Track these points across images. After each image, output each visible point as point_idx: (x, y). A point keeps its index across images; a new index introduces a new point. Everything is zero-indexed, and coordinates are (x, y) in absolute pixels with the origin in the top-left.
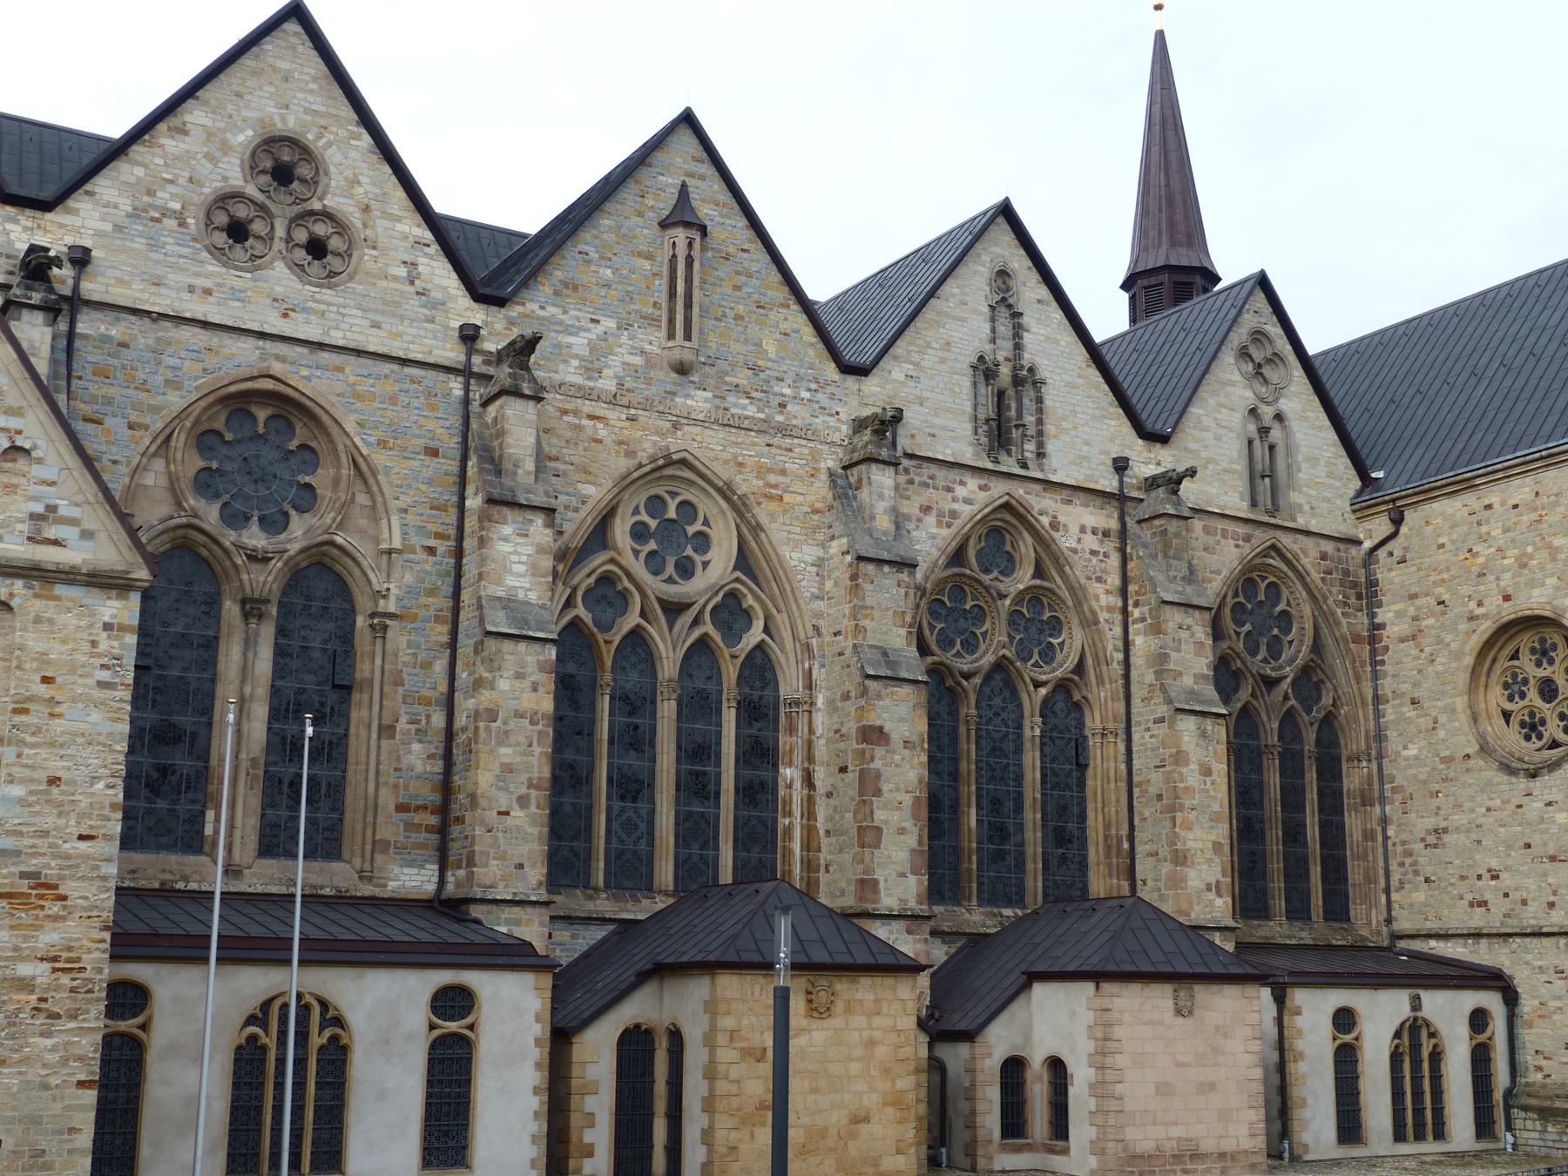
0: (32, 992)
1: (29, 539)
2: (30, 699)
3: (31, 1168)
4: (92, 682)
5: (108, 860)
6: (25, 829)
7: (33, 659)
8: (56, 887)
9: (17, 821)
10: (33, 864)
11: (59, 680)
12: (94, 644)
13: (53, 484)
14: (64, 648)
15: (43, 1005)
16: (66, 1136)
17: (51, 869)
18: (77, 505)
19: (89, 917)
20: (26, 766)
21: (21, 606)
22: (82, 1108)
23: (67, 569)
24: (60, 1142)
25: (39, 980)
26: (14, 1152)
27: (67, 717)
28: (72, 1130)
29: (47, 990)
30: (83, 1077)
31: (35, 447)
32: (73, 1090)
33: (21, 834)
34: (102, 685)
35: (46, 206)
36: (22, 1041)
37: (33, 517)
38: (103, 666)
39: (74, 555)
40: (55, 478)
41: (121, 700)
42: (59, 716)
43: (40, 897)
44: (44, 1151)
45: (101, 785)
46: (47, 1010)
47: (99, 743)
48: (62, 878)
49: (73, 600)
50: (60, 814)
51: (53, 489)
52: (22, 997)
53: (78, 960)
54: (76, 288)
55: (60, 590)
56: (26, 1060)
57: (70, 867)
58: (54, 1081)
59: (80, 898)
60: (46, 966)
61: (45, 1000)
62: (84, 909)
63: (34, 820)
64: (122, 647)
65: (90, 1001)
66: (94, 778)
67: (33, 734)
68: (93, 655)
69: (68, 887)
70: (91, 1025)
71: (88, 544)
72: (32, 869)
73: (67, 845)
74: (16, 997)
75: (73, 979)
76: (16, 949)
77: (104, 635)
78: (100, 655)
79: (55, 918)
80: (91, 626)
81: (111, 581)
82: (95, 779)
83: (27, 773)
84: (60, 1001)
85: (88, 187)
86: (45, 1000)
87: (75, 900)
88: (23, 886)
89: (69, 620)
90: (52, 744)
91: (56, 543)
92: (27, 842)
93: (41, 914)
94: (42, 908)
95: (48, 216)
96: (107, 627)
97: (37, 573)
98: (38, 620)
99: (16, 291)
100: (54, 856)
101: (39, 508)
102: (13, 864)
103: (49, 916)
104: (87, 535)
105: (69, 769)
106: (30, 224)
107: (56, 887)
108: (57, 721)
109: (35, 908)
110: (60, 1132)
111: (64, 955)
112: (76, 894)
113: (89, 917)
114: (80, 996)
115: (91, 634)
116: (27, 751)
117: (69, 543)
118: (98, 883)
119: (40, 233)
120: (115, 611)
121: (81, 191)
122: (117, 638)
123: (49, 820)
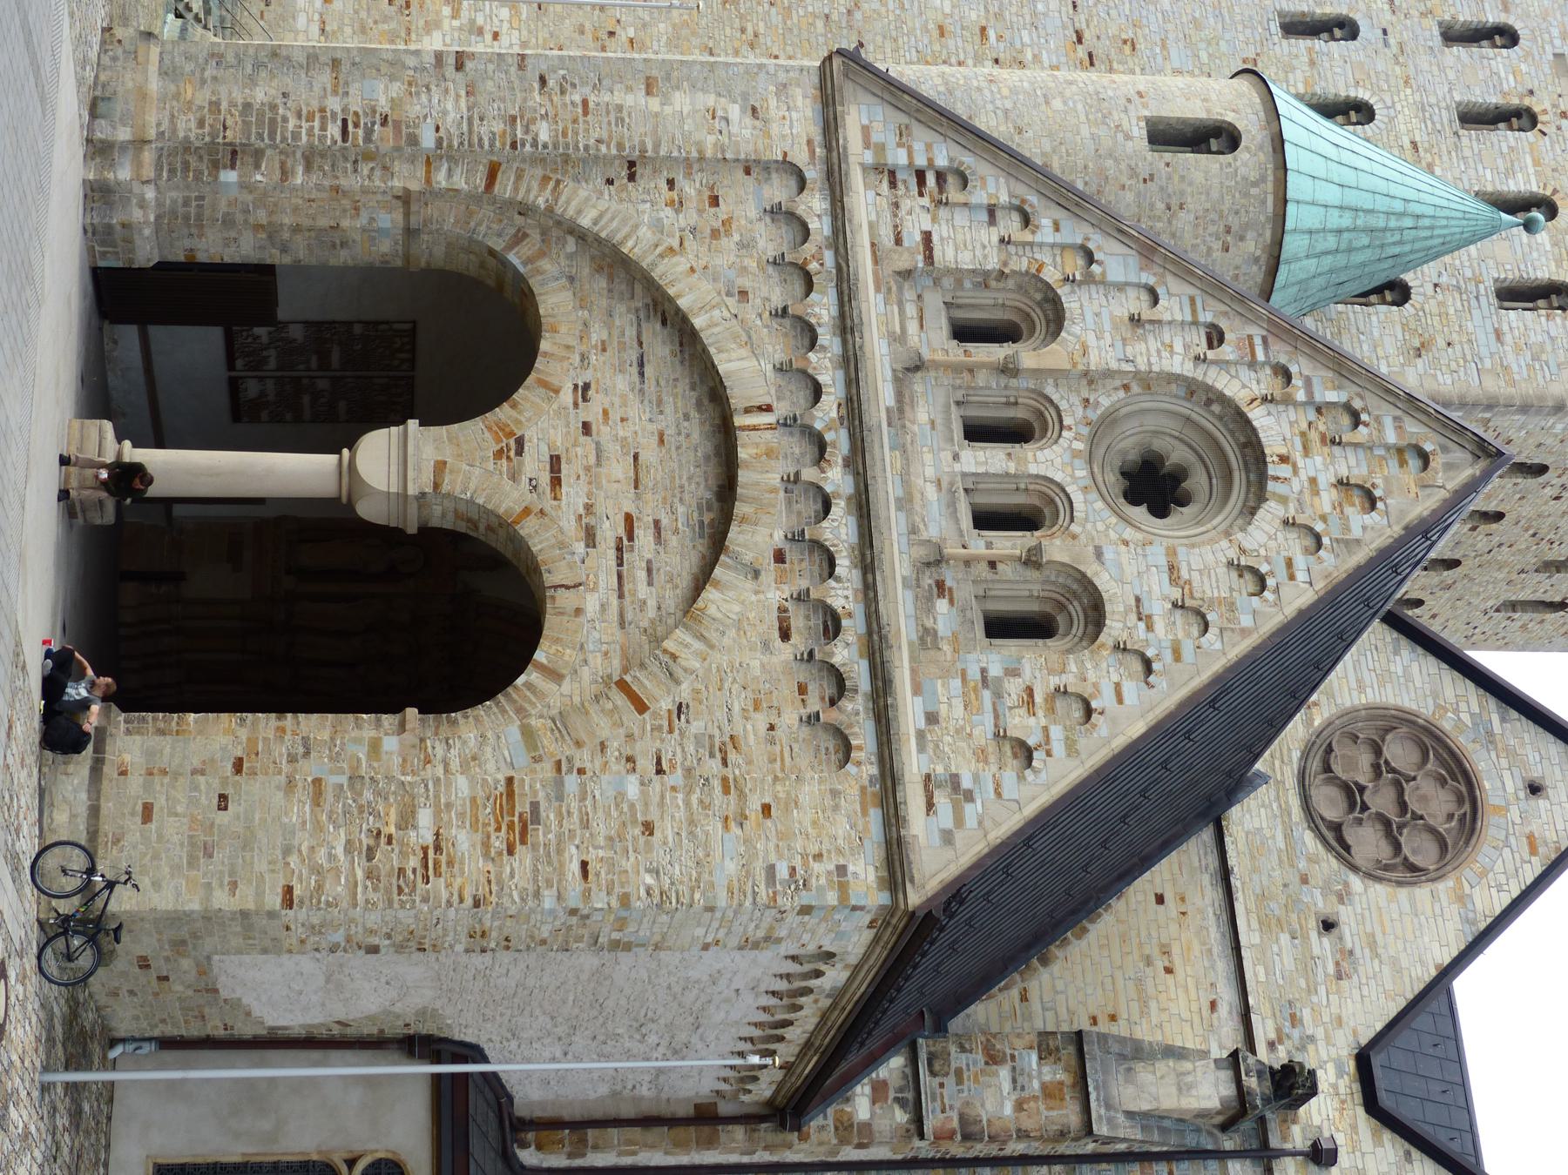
0: (399, 827)
1: (928, 777)
2: (742, 795)
3: (192, 844)
4: (773, 858)
5: (559, 897)
6: (589, 802)
7: (788, 793)
8: (523, 842)
9: (597, 794)
10: (549, 815)
11: (769, 823)
12: (818, 857)
13: (998, 794)
14: (807, 823)
15: (383, 840)
16: (227, 879)
17: (545, 835)
18: (980, 823)
19: (489, 882)
20: (663, 797)
21: (848, 774)
22: (259, 894)
23: (902, 813)
24: (221, 872)
25: (413, 834)
26: (212, 825)
27: (726, 836)
28: (234, 885)
29: (402, 843)
30: (297, 892)
31: (1036, 772)
32: (282, 882)
33: (583, 799)
34: (771, 870)
35: (1372, 1105)
36: (341, 820)
37: (955, 781)
38: (794, 869)
39: (918, 825)
40: (1005, 796)
41: (755, 894)
42: (726, 827)
43: (511, 826)
44: (211, 856)
45: (649, 880)
46: (378, 845)
47: (699, 874)
48: (535, 847)
49: (866, 829)
50: (611, 839)
51: (992, 795)
52: (393, 817)
53: (438, 874)
54: (1283, 1153)
55: (875, 815)
56: (318, 827)
57: (548, 855)
58: (293, 860)
59: (512, 870)
60: (429, 839)
61: (389, 842)
62: (499, 875)
63: (600, 813)
64: (820, 889)
65: (388, 891)
66: (658, 873)
67: (701, 802)
68: (804, 856)
69: (523, 853)
70: (359, 896)
71: (936, 840)
72: (543, 814)
73: (574, 850)
74: (393, 811)
75: (414, 871)
76: (449, 806)
77: (832, 867)
78: (805, 864)
79: (486, 845)
80: (840, 852)
81: (897, 864)
82: (656, 872)
83: (656, 799)
84: (387, 858)
85: (1416, 1154)
86: (389, 842)
87: (507, 863)
88: (523, 806)
89: (842, 827)
90: (692, 822)
91: (930, 805)
92: (574, 806)
93: (491, 829)
94: (498, 829)
95: (1361, 1111)
96: (841, 870)
97: (889, 783)
98: (835, 793)
99: (1251, 1060)
100: (560, 837)
101: (966, 783)
102: (548, 795)
103: (489, 837)
104: (947, 837)
105: (665, 843)
106: (1342, 1090)
107: (523, 842)
108: (720, 825)
109: (497, 821)
110: (232, 873)
111: (443, 859)
112: (516, 865)
113: (489, 882)
114: (394, 881)
115: (829, 852)
116: (680, 796)
117: (933, 818)
118: (531, 888)
119: (1336, 1104)
120: (863, 876)
121: (1407, 1145)
122: (830, 881)
123: (601, 828)
